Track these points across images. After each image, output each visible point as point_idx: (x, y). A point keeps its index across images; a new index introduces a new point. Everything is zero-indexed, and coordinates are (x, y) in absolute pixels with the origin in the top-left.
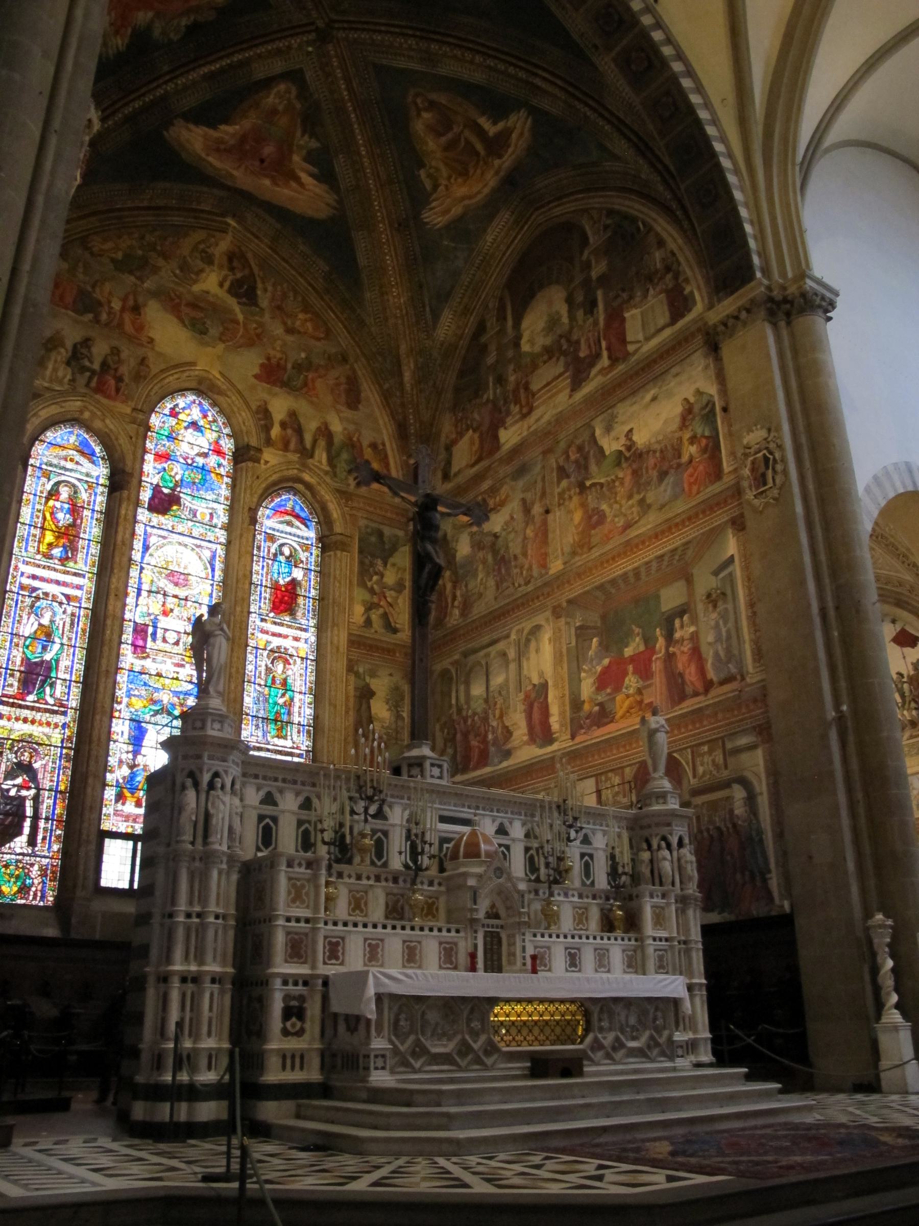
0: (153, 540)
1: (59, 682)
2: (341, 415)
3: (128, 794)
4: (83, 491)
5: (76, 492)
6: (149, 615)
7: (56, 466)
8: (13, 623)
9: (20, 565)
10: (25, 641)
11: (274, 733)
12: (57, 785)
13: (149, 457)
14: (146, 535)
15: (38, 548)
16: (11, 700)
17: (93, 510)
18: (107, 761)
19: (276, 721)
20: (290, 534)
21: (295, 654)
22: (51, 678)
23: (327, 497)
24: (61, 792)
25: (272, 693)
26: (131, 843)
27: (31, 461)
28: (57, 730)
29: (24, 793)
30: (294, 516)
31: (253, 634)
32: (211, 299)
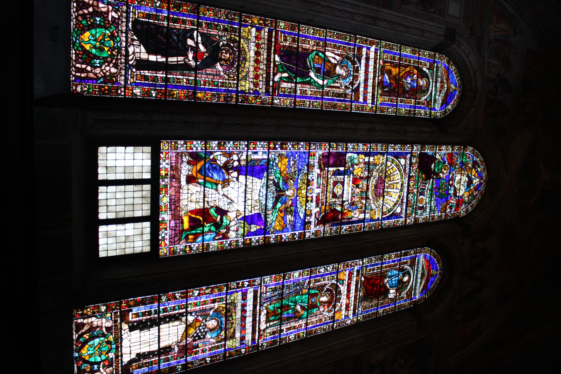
0: (403, 161)
1: (293, 85)
4: (426, 97)
6: (352, 166)
7: (437, 74)
8: (333, 41)
11: (271, 307)
12: (201, 89)
14: (403, 155)
16: (273, 40)
18: (229, 140)
24: (195, 94)
25: (304, 297)
26: (148, 176)
29: (191, 55)
30: (427, 278)
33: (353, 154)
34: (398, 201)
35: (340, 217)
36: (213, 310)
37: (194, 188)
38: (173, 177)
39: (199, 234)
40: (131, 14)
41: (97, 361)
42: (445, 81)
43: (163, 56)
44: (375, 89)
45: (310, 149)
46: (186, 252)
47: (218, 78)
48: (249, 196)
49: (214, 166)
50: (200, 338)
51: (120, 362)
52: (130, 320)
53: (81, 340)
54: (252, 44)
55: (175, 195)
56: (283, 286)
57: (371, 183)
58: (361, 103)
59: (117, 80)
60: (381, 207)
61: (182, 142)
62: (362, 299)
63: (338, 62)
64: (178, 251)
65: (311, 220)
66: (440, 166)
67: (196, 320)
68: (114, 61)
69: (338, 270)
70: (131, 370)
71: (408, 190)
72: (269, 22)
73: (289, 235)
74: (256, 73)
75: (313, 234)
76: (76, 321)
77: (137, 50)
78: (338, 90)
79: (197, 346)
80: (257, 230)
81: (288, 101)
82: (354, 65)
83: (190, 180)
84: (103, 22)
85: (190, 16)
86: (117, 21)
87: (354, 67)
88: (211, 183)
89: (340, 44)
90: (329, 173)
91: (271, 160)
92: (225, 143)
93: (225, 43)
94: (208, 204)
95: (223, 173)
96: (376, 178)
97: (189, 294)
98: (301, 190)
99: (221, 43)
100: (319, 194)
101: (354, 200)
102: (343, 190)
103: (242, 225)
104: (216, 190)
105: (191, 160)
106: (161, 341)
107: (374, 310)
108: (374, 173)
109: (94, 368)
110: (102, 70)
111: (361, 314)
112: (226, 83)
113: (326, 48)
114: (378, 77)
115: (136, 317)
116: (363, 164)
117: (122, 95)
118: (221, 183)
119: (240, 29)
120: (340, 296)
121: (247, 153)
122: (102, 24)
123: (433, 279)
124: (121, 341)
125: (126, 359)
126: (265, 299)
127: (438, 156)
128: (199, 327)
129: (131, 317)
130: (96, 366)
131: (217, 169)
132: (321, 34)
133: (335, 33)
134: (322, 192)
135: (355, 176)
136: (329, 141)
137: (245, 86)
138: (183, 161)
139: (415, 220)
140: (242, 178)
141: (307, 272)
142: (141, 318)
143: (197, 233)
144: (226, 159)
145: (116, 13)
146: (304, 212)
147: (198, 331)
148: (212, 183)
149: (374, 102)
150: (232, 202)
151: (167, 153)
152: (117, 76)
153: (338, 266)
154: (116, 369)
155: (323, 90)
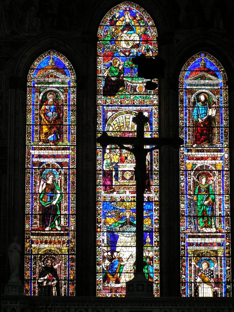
0: (109, 114)
1: (62, 216)
4: (61, 94)
5: (57, 96)
6: (112, 164)
7: (42, 83)
8: (32, 187)
9: (31, 151)
10: (40, 196)
11: (202, 224)
12: (69, 276)
13: (100, 59)
14: (105, 112)
15: (40, 137)
16: (37, 232)
17: (69, 105)
19: (203, 217)
20: (204, 85)
21: (214, 169)
24: (71, 280)
25: (199, 199)
27: (28, 84)
28: (65, 245)
31: (183, 162)
36: (196, 266)
38: (116, 292)
39: (149, 275)
44: (59, 148)
46: (158, 283)
47: (62, 267)
49: (110, 267)
50: (212, 274)
54: (41, 246)
56: (189, 216)
58: (70, 159)
61: (98, 286)
63: (44, 182)
65: (147, 197)
67: (200, 276)
69: (184, 170)
72: (27, 235)
75: (156, 194)
78: (62, 181)
79: (217, 275)
85: (31, 285)
87: (47, 168)
88: (120, 269)
89: (33, 181)
90: (116, 184)
91: (107, 230)
92: (98, 261)
93: (42, 263)
94: (131, 270)
95: (114, 262)
97: (183, 281)
99: (43, 266)
100: (130, 192)
102: (128, 171)
104: (124, 265)
105: (107, 281)
107: (222, 130)
111: (222, 143)
112: (64, 262)
113: (37, 192)
114: (51, 145)
116: (111, 155)
118: (120, 263)
119: (34, 255)
121: (103, 246)
123: (208, 64)
126: (195, 229)
127: (105, 74)
128: (205, 274)
131: (112, 265)
132: (28, 198)
133: (27, 186)
134: (129, 189)
136: (95, 185)
137: (65, 250)
138: (107, 286)
140: (118, 249)
141: (182, 197)
143: (148, 277)
144: (107, 260)
147: (208, 275)
148: (120, 268)
149: (68, 148)
155: (63, 193)
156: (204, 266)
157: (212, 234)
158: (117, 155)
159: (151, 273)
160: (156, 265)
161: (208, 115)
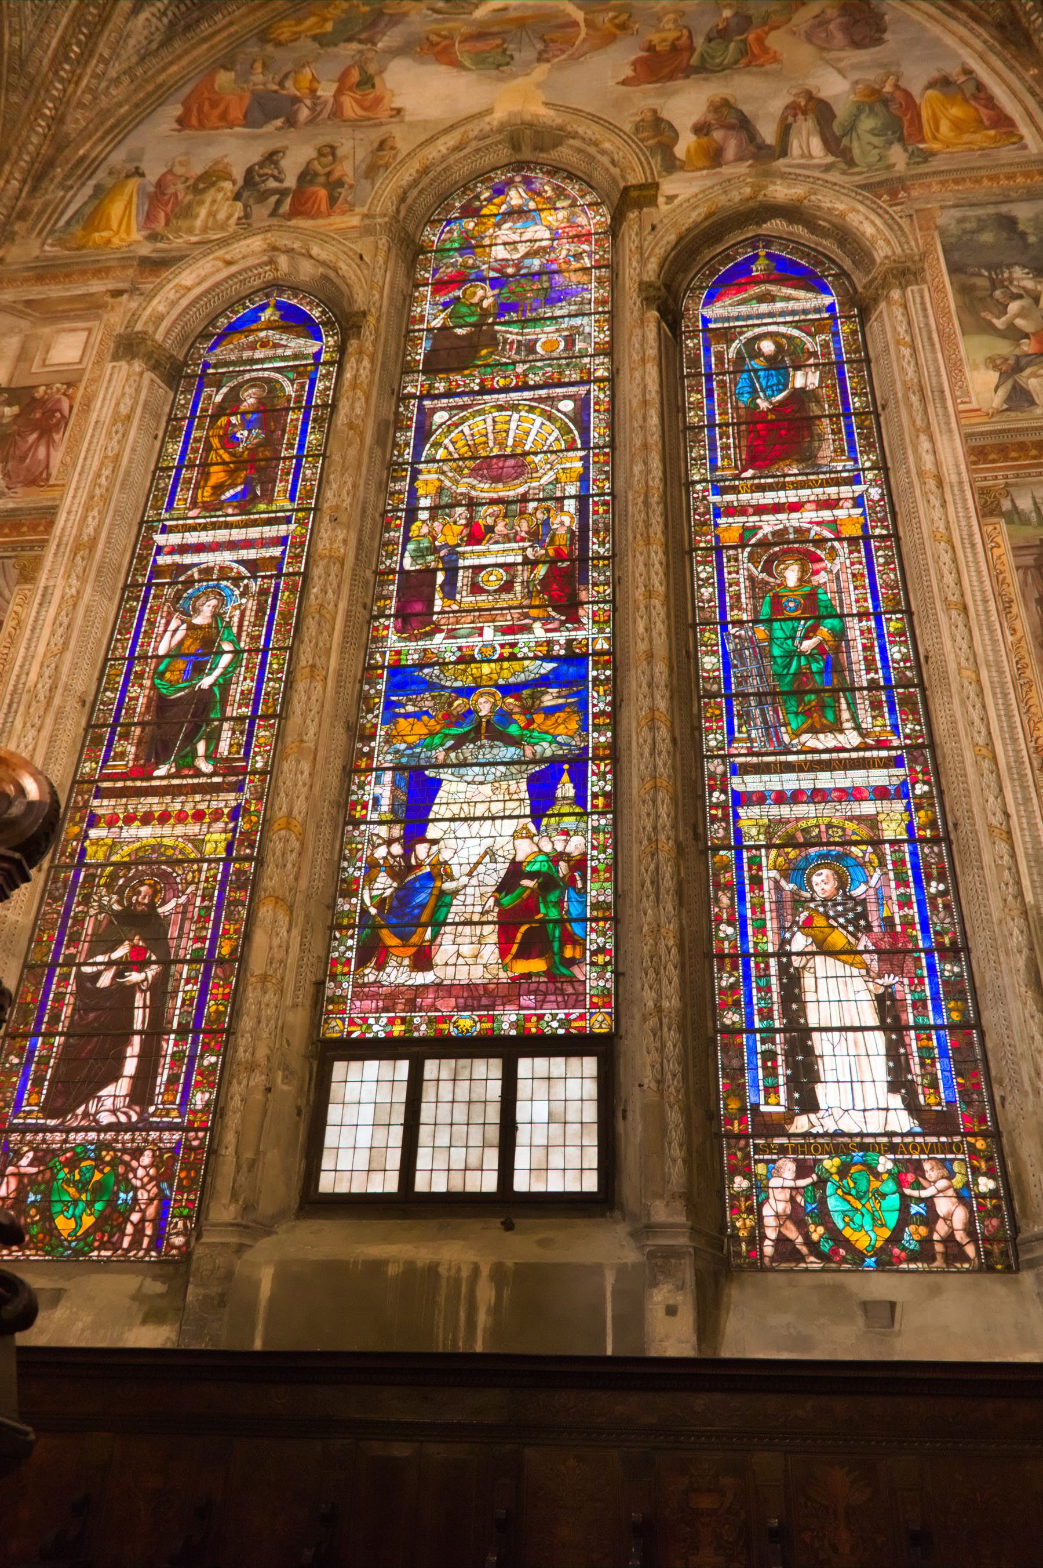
0: (440, 417)
1: (226, 726)
2: (841, 65)
3: (390, 939)
4: (286, 384)
6: (435, 550)
7: (233, 363)
14: (425, 415)
16: (120, 784)
19: (798, 693)
20: (771, 315)
22: (209, 722)
23: (841, 207)
24: (221, 961)
25: (778, 634)
26: (403, 1067)
28: (220, 825)
29: (134, 977)
32: (512, 14)
33: (407, 554)
34: (543, 413)
35: (566, 564)
36: (783, 883)
37: (444, 953)
40: (29, 1121)
41: (897, 1206)
42: (251, 338)
43: (128, 1042)
45: (382, 667)
46: (606, 964)
47: (191, 908)
48: (480, 810)
50: (864, 915)
51: (909, 1140)
52: (782, 1109)
53: (826, 1247)
54: (124, 834)
55: (457, 998)
57: (486, 495)
59: (169, 1150)
60: (554, 457)
61: (332, 985)
62: (807, 467)
63: (183, 622)
64: (601, 983)
65: (563, 641)
66: (464, 310)
68: (127, 1158)
70: (939, 1108)
71: (517, 389)
73: (595, 695)
74: (190, 819)
75: (601, 631)
76: (767, 1260)
77: (108, 1104)
78: (248, 613)
79: (889, 922)
80: (572, 781)
81: (263, 733)
82: (194, 581)
83: (423, 960)
84: (39, 1185)
86: (40, 1154)
87: (200, 581)
88: (437, 908)
93: (115, 897)
94: (487, 912)
96: (475, 482)
98: (481, 677)
99: (116, 907)
100: (497, 629)
101: (523, 534)
103: (553, 820)
104: (455, 893)
106: (857, 1024)
108: (462, 489)
109: (918, 1213)
110: (143, 1187)
115: (777, 1092)
117: (205, 1137)
120: (791, 530)
122: (43, 1187)
124: (843, 1134)
125: (902, 1122)
126: (770, 740)
127: (437, 323)
128: (828, 917)
129: (775, 1107)
130: (914, 1209)
134: (493, 621)
135: (461, 540)
138: (375, 982)
139: (599, 355)
140: (433, 831)
142: (781, 1080)
144: (382, 874)
145: (22, 1156)
146: (539, 662)
147: (841, 920)
150: (491, 853)
151: (352, 1023)
152: (160, 1149)
153: (702, 549)
154: (931, 1152)
155: (244, 651)
156: (823, 882)
157: (846, 755)
158: (455, 523)
159: (575, 920)
160: (597, 885)
161: (793, 387)
